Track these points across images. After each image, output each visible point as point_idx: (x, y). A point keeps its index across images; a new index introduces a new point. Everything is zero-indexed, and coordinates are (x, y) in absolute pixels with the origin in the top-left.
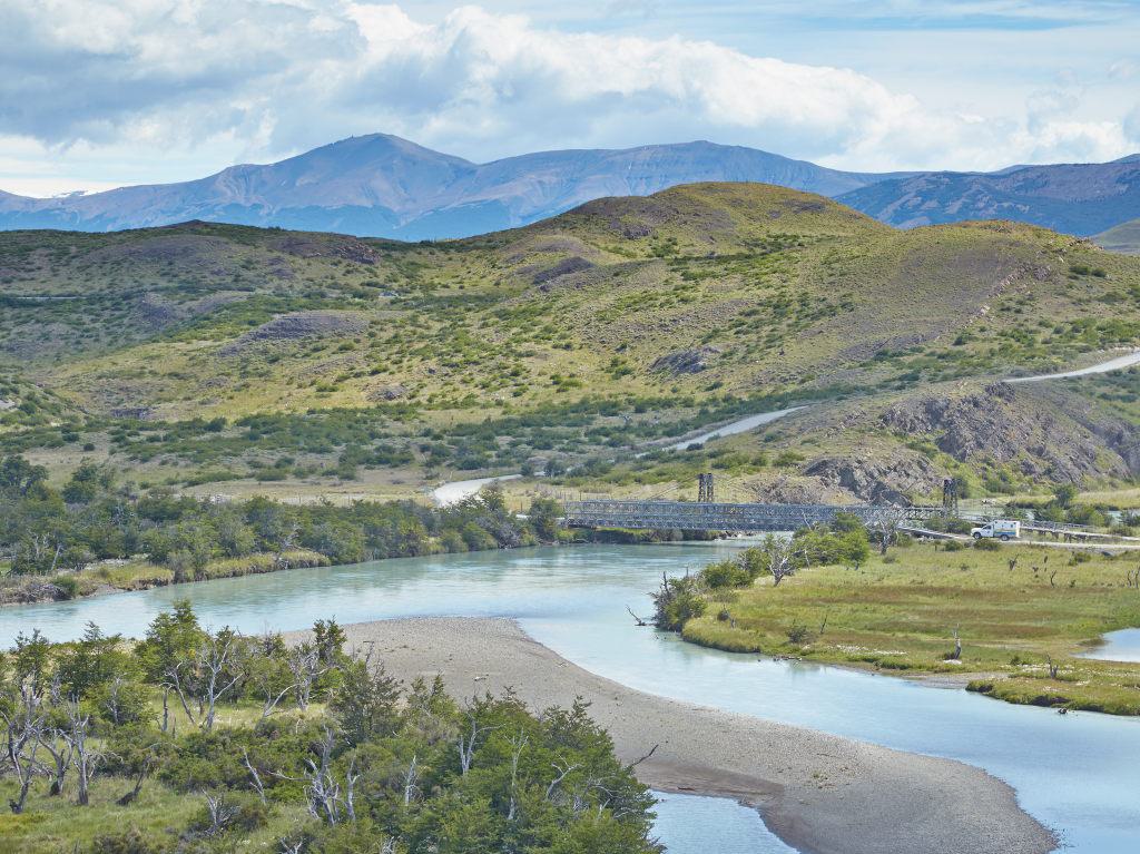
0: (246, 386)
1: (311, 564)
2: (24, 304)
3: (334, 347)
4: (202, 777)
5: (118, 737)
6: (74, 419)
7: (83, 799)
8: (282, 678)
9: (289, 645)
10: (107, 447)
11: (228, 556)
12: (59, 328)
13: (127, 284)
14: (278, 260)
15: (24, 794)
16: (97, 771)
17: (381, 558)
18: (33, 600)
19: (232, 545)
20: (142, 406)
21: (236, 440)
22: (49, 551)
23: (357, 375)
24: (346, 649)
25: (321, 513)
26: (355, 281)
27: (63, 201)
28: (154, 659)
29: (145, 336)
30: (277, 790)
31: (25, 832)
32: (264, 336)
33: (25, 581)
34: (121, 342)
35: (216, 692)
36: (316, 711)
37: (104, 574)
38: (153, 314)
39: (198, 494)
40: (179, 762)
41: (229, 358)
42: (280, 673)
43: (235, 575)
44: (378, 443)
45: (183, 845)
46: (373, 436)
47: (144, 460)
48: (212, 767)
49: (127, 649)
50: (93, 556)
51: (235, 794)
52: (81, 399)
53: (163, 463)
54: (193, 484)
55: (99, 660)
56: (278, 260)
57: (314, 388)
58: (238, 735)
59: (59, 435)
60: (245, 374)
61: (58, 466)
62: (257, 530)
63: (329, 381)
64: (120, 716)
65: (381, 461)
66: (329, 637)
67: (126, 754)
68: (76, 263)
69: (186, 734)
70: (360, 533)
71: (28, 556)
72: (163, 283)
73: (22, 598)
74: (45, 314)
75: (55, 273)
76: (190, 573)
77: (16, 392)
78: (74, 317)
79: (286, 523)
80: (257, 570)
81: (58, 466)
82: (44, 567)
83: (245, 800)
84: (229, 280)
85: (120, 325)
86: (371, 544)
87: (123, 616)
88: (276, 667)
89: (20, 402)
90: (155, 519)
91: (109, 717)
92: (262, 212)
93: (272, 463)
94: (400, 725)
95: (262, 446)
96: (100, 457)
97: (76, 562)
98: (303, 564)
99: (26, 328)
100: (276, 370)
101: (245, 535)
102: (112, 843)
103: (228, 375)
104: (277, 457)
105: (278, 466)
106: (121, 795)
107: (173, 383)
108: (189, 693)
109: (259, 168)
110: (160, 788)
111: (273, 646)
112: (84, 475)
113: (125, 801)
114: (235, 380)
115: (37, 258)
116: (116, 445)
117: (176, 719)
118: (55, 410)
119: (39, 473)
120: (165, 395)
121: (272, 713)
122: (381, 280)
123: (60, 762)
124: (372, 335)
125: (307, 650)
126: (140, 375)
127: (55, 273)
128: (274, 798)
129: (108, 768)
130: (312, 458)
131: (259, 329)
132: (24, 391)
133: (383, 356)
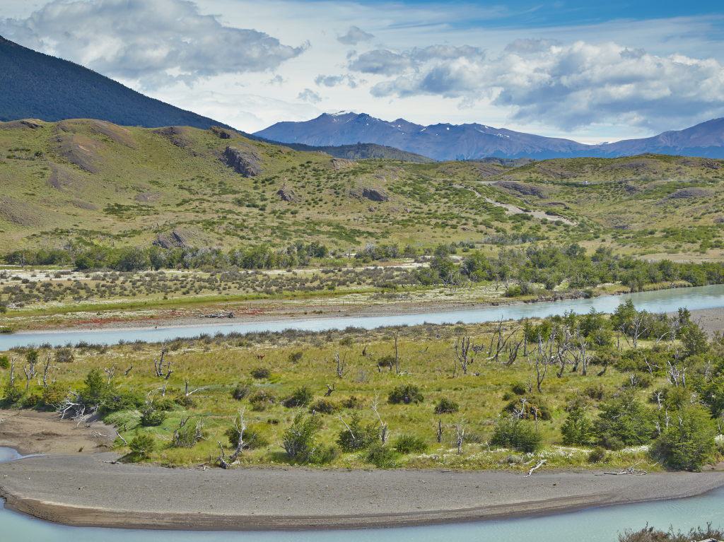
0: (666, 217)
1: (685, 286)
2: (581, 186)
3: (701, 201)
4: (630, 366)
5: (599, 351)
6: (599, 230)
7: (584, 373)
8: (665, 329)
9: (669, 317)
10: (610, 240)
11: (652, 282)
12: (594, 195)
13: (621, 178)
14: (680, 168)
15: (562, 371)
16: (591, 363)
17: (713, 284)
18: (576, 298)
19: (653, 278)
20: (625, 225)
21: (660, 237)
22: (583, 280)
23: (710, 213)
24: (690, 319)
25: (689, 267)
26: (710, 176)
27: (600, 146)
28: (617, 322)
29: (627, 198)
30: (658, 372)
31: (562, 385)
32: (673, 198)
33: (574, 291)
34: (618, 200)
35: (638, 334)
36: (677, 343)
37: (604, 289)
38: (631, 189)
39: (643, 258)
40: (622, 360)
41: (659, 206)
42: (664, 328)
43: (655, 290)
44: (716, 239)
45: (619, 391)
46: (714, 237)
47: (624, 246)
48: (634, 363)
49: (607, 318)
50: (600, 282)
51: (641, 373)
52: (602, 222)
53: (631, 247)
54: (642, 255)
55: (595, 321)
56: (680, 168)
57: (692, 218)
58: (645, 351)
59: (592, 235)
60: (665, 212)
61: (590, 248)
62: (664, 272)
63: (698, 215)
64: (602, 342)
65: (716, 246)
66: (684, 314)
67: (602, 357)
68: (601, 170)
69: (626, 350)
70: (705, 275)
71: (575, 282)
72: (634, 177)
73: (572, 297)
74: (588, 189)
75: (593, 174)
76: (637, 289)
77: (577, 219)
78: (600, 190)
79: (675, 270)
80: (663, 288)
81: (590, 248)
82: (582, 286)
83: (644, 376)
84: (660, 176)
85: (618, 194)
86: (709, 279)
87: (607, 305)
88: (663, 325)
89: (579, 223)
90: (626, 268)
91: (597, 343)
92: (677, 149)
93: (674, 247)
94: (708, 349)
95: (670, 240)
96: (607, 245)
97: (594, 284)
98: (681, 286)
99: (582, 195)
100: (678, 211)
101: (659, 274)
102: (591, 390)
103: (659, 213)
104: (676, 244)
105: (676, 248)
106: (599, 372)
107: (638, 216)
108: (630, 335)
109: (676, 132)
110: (614, 370)
111: (663, 317)
112: (600, 251)
113: (600, 375)
114: (661, 215)
115: (587, 168)
116: (614, 240)
117: (623, 344)
118: (592, 226)
119: (583, 250)
120: (634, 220)
121: (659, 343)
122: (720, 175)
123: (576, 359)
124: (716, 197)
125: (675, 319)
126: (625, 213)
127: (593, 174)
128: (657, 376)
129: (595, 362)
130: (690, 245)
131: (671, 195)
132: (580, 219)
133: (720, 205)
